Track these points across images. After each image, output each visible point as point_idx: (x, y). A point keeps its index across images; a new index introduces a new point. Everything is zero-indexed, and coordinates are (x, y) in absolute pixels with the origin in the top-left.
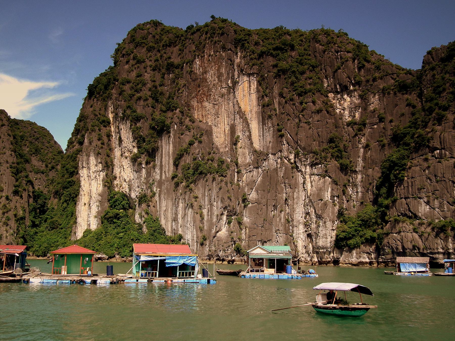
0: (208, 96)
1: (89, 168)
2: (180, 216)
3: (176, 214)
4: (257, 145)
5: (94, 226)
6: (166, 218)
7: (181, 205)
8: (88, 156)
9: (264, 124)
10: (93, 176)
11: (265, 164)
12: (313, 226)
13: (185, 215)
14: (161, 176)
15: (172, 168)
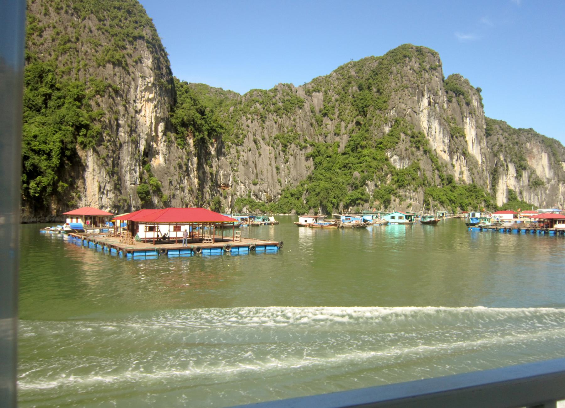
0: (534, 158)
1: (503, 180)
2: (532, 198)
3: (531, 197)
4: (548, 176)
5: (505, 201)
6: (526, 198)
7: (532, 195)
8: (503, 175)
9: (550, 169)
10: (504, 183)
11: (551, 183)
12: (562, 201)
13: (534, 198)
14: (523, 184)
15: (527, 182)
